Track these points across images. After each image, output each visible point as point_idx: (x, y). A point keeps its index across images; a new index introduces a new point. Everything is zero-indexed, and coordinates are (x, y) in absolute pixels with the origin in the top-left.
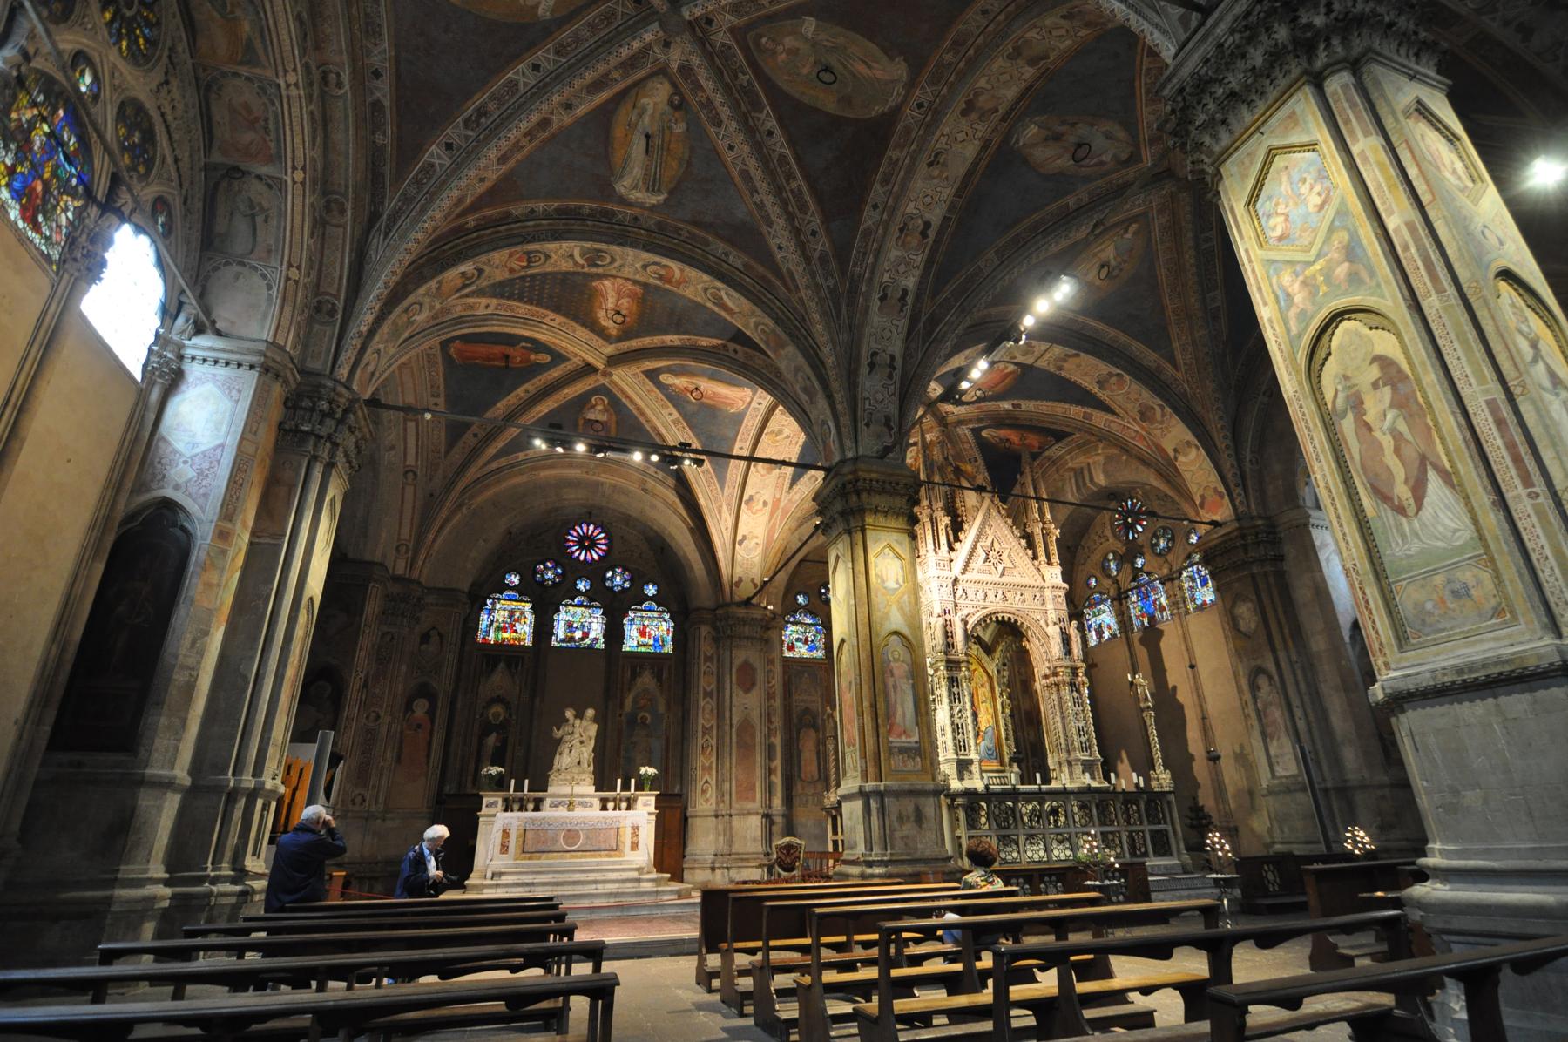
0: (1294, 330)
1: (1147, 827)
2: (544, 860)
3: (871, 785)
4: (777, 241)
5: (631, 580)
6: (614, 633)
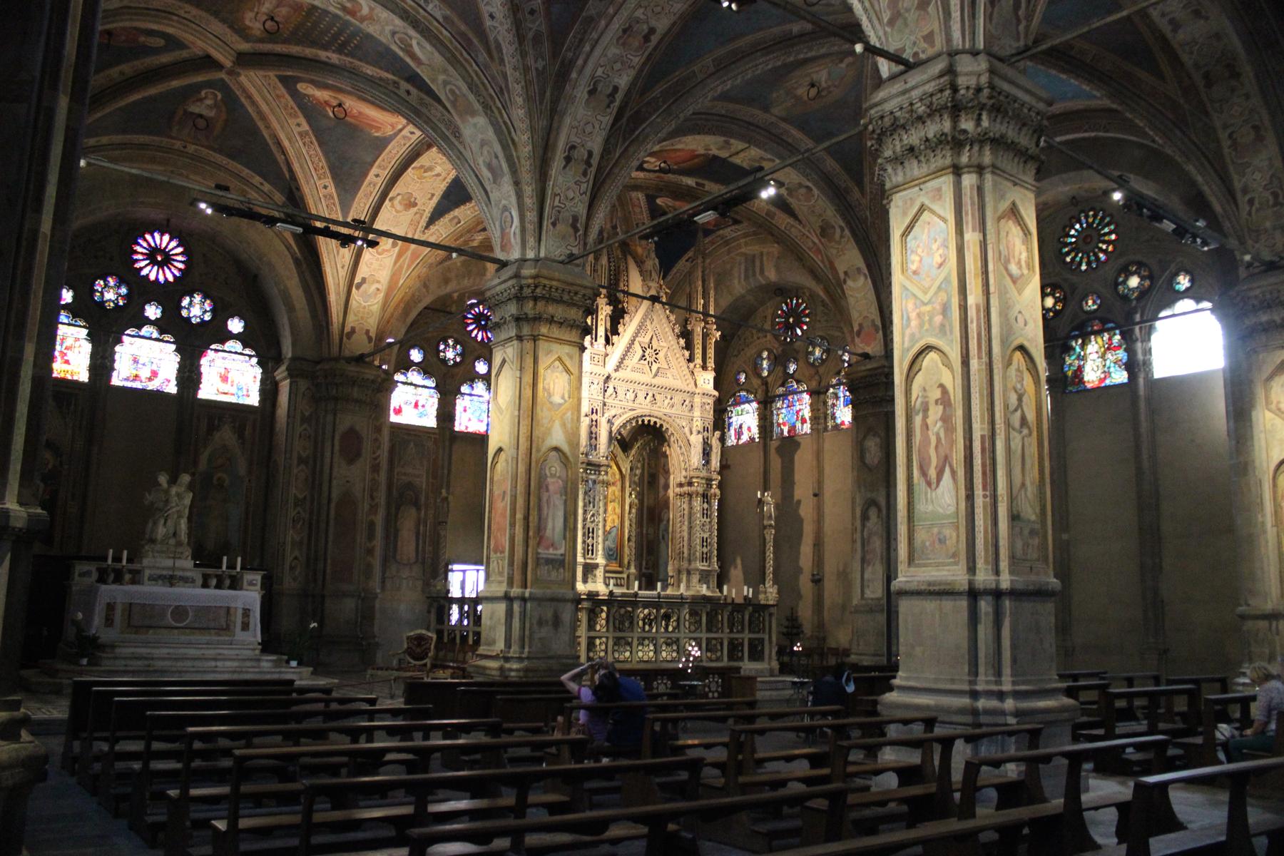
0: (906, 345)
1: (746, 636)
2: (151, 635)
3: (516, 591)
4: (491, 10)
5: (213, 311)
6: (189, 375)
